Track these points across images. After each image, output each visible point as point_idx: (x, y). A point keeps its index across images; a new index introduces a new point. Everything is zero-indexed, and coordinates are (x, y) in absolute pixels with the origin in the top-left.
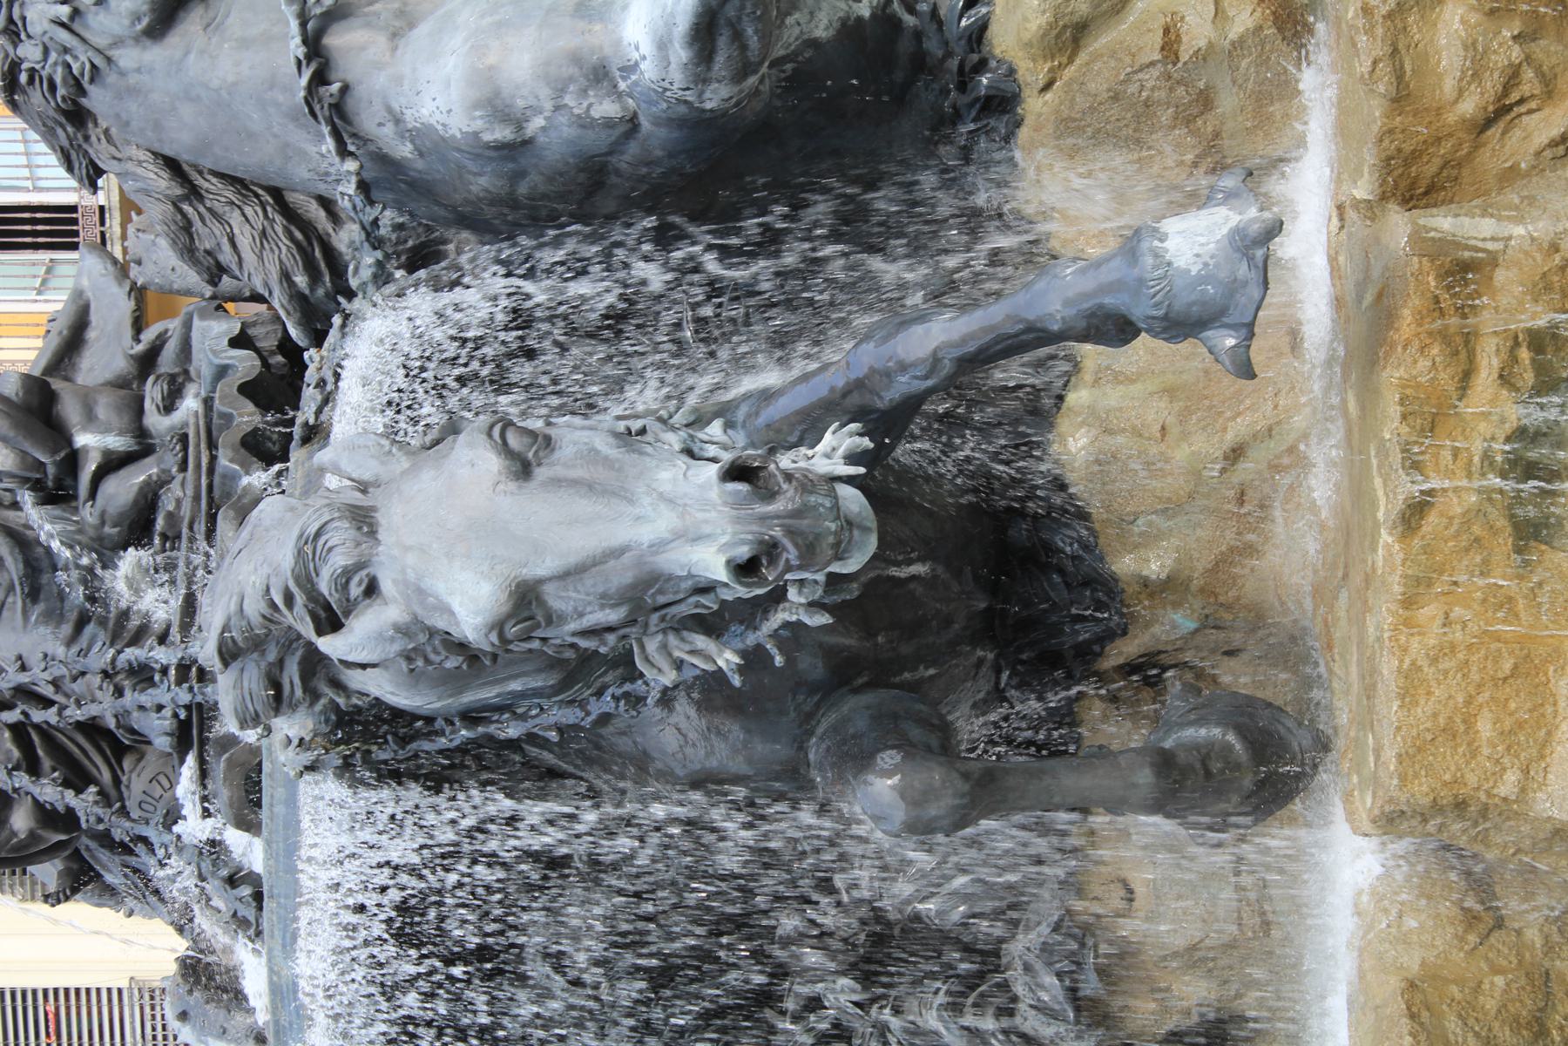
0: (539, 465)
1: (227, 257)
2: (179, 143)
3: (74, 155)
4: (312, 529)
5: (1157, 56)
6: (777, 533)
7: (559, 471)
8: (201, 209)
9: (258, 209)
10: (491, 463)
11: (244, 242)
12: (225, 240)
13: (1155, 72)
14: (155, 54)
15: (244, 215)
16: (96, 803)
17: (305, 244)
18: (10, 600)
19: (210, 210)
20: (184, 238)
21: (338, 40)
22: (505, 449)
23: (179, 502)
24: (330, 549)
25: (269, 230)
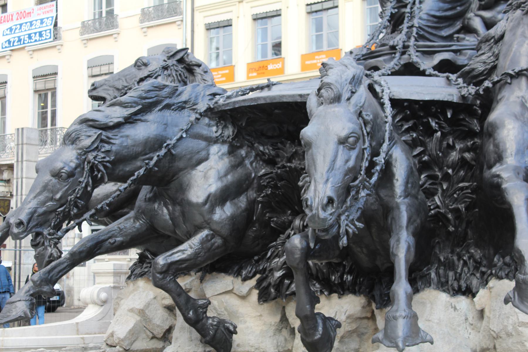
0: (344, 147)
1: (480, 52)
2: (506, 38)
4: (332, 87)
5: (520, 320)
6: (314, 212)
7: (340, 152)
8: (492, 44)
9: (493, 60)
10: (343, 134)
11: (484, 57)
12: (483, 52)
13: (516, 321)
15: (491, 56)
16: (385, 25)
17: (472, 74)
20: (484, 40)
22: (347, 137)
23: (468, 40)
24: (328, 92)
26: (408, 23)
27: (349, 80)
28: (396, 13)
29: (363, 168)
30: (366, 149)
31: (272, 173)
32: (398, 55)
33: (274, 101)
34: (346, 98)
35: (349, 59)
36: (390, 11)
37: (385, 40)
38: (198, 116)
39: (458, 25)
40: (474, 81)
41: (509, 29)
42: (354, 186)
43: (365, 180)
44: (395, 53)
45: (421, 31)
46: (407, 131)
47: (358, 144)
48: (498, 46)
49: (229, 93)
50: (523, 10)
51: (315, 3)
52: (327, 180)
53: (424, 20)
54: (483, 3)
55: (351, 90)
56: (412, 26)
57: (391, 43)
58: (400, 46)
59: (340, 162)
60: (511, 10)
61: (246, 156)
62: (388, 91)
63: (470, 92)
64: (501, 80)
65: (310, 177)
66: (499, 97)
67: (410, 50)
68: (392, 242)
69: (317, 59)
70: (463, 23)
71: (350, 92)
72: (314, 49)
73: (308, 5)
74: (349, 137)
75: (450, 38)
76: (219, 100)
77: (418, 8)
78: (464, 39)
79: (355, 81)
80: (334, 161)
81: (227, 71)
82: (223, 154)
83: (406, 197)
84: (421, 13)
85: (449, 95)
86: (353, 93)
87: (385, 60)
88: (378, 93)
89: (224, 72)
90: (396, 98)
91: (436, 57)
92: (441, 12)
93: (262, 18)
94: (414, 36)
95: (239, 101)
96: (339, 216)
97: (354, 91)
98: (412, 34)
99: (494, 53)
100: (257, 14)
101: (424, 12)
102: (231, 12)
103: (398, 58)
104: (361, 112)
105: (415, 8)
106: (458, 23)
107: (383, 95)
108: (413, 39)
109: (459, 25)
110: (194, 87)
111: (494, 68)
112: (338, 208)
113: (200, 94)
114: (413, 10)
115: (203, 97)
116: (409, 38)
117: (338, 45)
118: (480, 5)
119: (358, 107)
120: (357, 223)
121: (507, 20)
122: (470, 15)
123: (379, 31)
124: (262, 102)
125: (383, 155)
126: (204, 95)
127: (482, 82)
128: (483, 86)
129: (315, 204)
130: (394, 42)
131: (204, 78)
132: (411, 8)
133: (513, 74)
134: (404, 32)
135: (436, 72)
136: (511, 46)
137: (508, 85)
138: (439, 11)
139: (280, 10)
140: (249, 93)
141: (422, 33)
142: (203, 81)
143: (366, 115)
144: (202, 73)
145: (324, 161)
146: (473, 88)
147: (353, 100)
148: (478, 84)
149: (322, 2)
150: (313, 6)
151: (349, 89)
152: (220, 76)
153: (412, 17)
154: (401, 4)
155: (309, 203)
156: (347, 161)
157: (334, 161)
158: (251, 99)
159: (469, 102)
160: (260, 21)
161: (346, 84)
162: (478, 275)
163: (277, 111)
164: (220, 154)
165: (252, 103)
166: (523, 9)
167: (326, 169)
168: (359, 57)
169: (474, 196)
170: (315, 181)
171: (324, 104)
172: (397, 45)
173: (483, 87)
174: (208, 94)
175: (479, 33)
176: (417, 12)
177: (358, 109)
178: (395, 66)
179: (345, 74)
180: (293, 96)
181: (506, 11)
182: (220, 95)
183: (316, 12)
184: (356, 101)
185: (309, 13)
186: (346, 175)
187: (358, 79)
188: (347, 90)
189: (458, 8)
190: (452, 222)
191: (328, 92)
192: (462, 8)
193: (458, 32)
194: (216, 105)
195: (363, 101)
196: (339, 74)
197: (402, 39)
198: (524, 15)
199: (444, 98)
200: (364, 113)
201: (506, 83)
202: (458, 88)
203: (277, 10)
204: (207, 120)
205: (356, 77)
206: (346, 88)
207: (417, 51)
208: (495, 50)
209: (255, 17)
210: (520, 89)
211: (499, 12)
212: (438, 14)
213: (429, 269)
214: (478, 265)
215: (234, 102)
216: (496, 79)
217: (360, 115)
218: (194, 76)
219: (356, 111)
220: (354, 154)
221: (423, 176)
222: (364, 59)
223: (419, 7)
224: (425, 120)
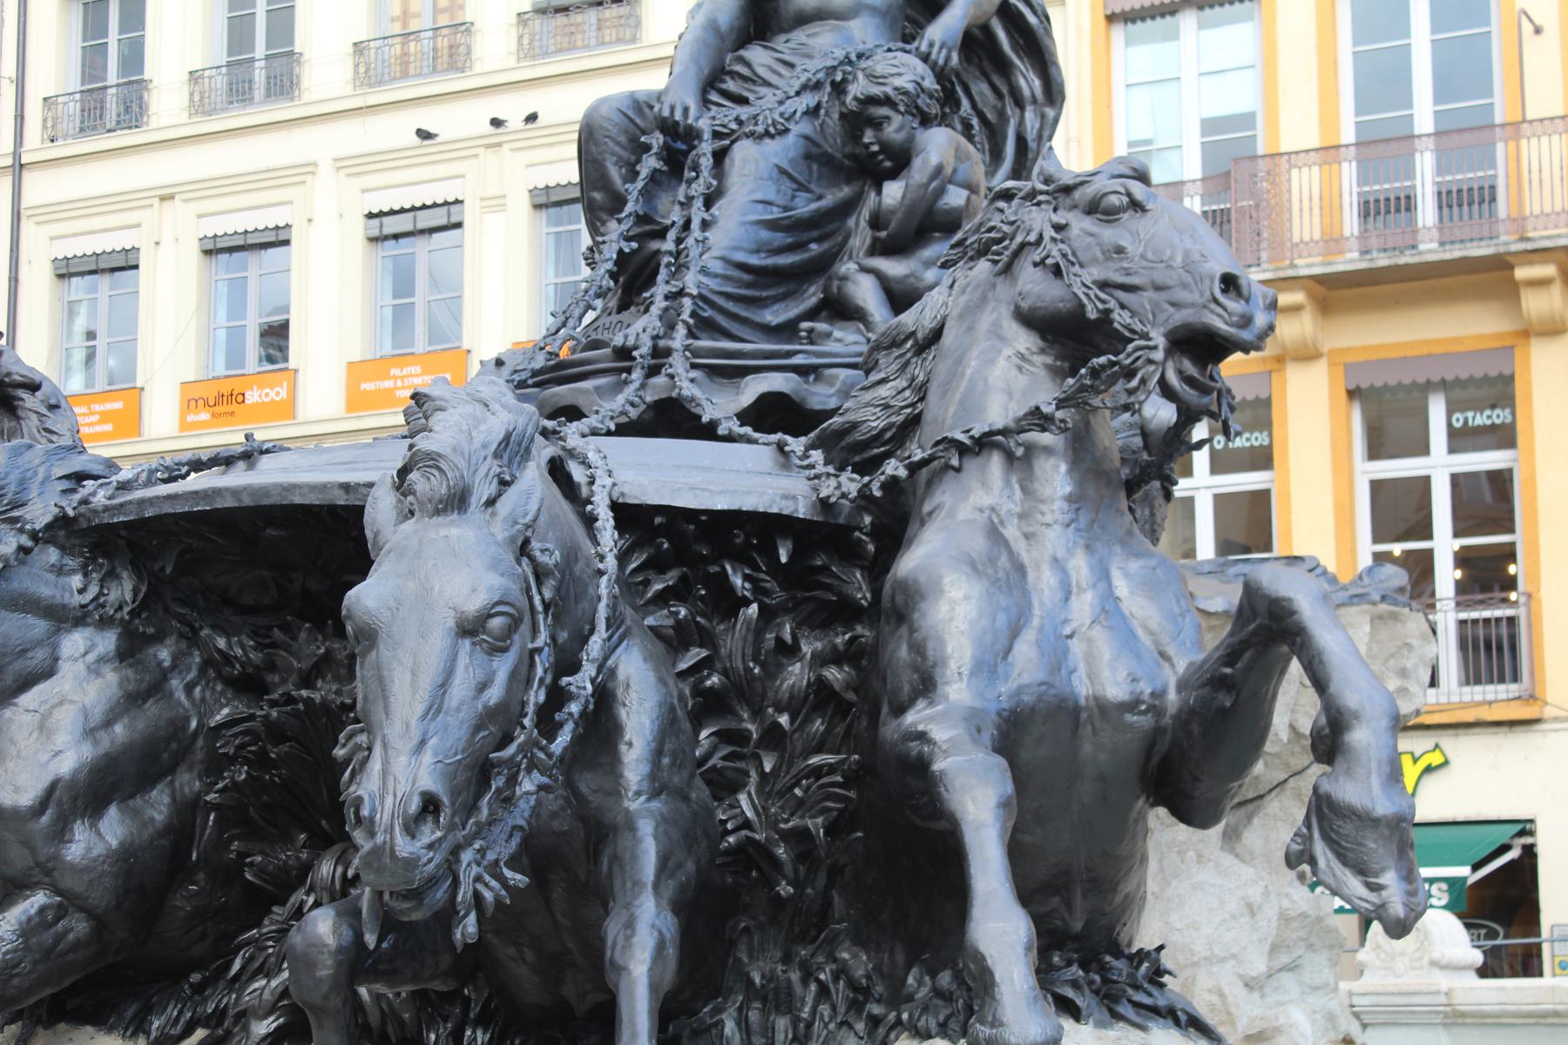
0: (474, 644)
1: (874, 377)
2: (948, 338)
3: (961, 249)
4: (443, 465)
6: (380, 838)
7: (463, 660)
8: (909, 355)
9: (909, 401)
10: (474, 604)
11: (884, 391)
12: (882, 375)
14: (1005, 312)
15: (904, 390)
16: (601, 287)
17: (849, 439)
18: (775, 209)
19: (908, 363)
20: (886, 341)
21: (995, 463)
23: (839, 340)
24: (429, 479)
25: (891, 411)
26: (667, 282)
27: (494, 446)
28: (633, 252)
29: (531, 709)
30: (539, 650)
31: (252, 717)
32: (637, 375)
33: (266, 502)
34: (484, 499)
35: (493, 382)
36: (615, 247)
37: (600, 330)
38: (25, 541)
39: (812, 296)
40: (857, 459)
41: (955, 312)
42: (501, 763)
43: (537, 744)
44: (629, 371)
45: (706, 307)
46: (662, 599)
47: (516, 637)
48: (925, 359)
49: (125, 474)
50: (995, 262)
51: (392, 212)
52: (423, 743)
53: (716, 276)
54: (883, 234)
55: (498, 475)
56: (681, 293)
57: (618, 340)
58: (645, 349)
59: (460, 689)
60: (961, 258)
61: (174, 666)
62: (609, 482)
63: (844, 489)
64: (931, 459)
65: (369, 733)
66: (926, 508)
67: (674, 363)
68: (613, 929)
69: (395, 378)
70: (826, 290)
71: (495, 481)
72: (388, 349)
73: (371, 216)
74: (490, 616)
75: (787, 330)
76: (94, 494)
77: (697, 241)
78: (828, 335)
79: (512, 449)
80: (444, 686)
81: (118, 405)
82: (101, 660)
83: (654, 794)
84: (704, 257)
85: (785, 497)
86: (505, 484)
87: (597, 389)
88: (579, 484)
89: (108, 406)
90: (630, 501)
91: (747, 385)
92: (763, 255)
93: (231, 250)
94: (683, 321)
95: (158, 497)
96: (456, 851)
97: (508, 478)
98: (679, 315)
99: (913, 380)
100: (215, 236)
101: (715, 252)
102: (138, 225)
103: (636, 385)
104: (526, 542)
105: (690, 241)
106: (812, 289)
107: (592, 493)
108: (681, 331)
109: (814, 294)
110: (16, 453)
111: (914, 422)
112: (451, 827)
113: (36, 473)
114: (682, 246)
115: (43, 482)
116: (671, 327)
117: (459, 338)
118: (875, 240)
119: (518, 527)
120: (508, 873)
121: (951, 287)
122: (847, 267)
123: (582, 304)
124: (230, 503)
125: (589, 670)
126: (46, 479)
127: (878, 461)
128: (883, 473)
129: (383, 818)
130: (626, 337)
131: (48, 425)
132: (679, 241)
133: (967, 441)
134: (655, 310)
135: (748, 430)
136: (960, 361)
137: (951, 473)
138: (758, 251)
139: (288, 226)
140: (188, 474)
141: (708, 313)
142: (44, 434)
143: (542, 551)
144: (44, 410)
145: (414, 684)
146: (852, 480)
147: (504, 506)
148: (868, 467)
149: (413, 209)
150: (386, 220)
151: (491, 474)
152: (95, 418)
153: (680, 268)
154: (648, 228)
155: (365, 812)
156: (483, 687)
157: (444, 686)
158: (195, 495)
159: (841, 521)
160: (224, 257)
161: (485, 458)
162: (860, 1026)
163: (271, 532)
164: (91, 657)
165: (197, 505)
166: (997, 258)
167: (420, 709)
168: (523, 376)
169: (852, 794)
170: (385, 746)
171: (417, 514)
172: (636, 348)
173: (883, 478)
174: (60, 474)
175: (870, 319)
176: (694, 252)
177: (519, 531)
178: (629, 408)
179: (483, 427)
180: (324, 487)
181: (947, 261)
182: (96, 478)
183: (396, 237)
184: (514, 510)
185: (373, 240)
186: (478, 728)
187: (520, 444)
188: (487, 475)
189: (813, 246)
190: (788, 869)
191: (429, 479)
192: (826, 245)
193: (811, 315)
194: (83, 509)
195: (533, 508)
196: (465, 427)
197: (649, 330)
198: (999, 274)
199: (771, 507)
200: (535, 545)
201: (948, 467)
202: (809, 479)
203: (277, 228)
204: (53, 555)
205: (513, 438)
206: (483, 470)
207: (694, 366)
208: (917, 372)
209: (210, 246)
210: (985, 484)
211: (928, 264)
212: (754, 260)
213: (719, 1010)
214: (860, 995)
215: (142, 502)
216: (918, 455)
217: (524, 549)
218: (18, 418)
219: (512, 540)
220: (503, 667)
221: (704, 734)
222: (536, 385)
223: (700, 239)
224: (714, 569)
